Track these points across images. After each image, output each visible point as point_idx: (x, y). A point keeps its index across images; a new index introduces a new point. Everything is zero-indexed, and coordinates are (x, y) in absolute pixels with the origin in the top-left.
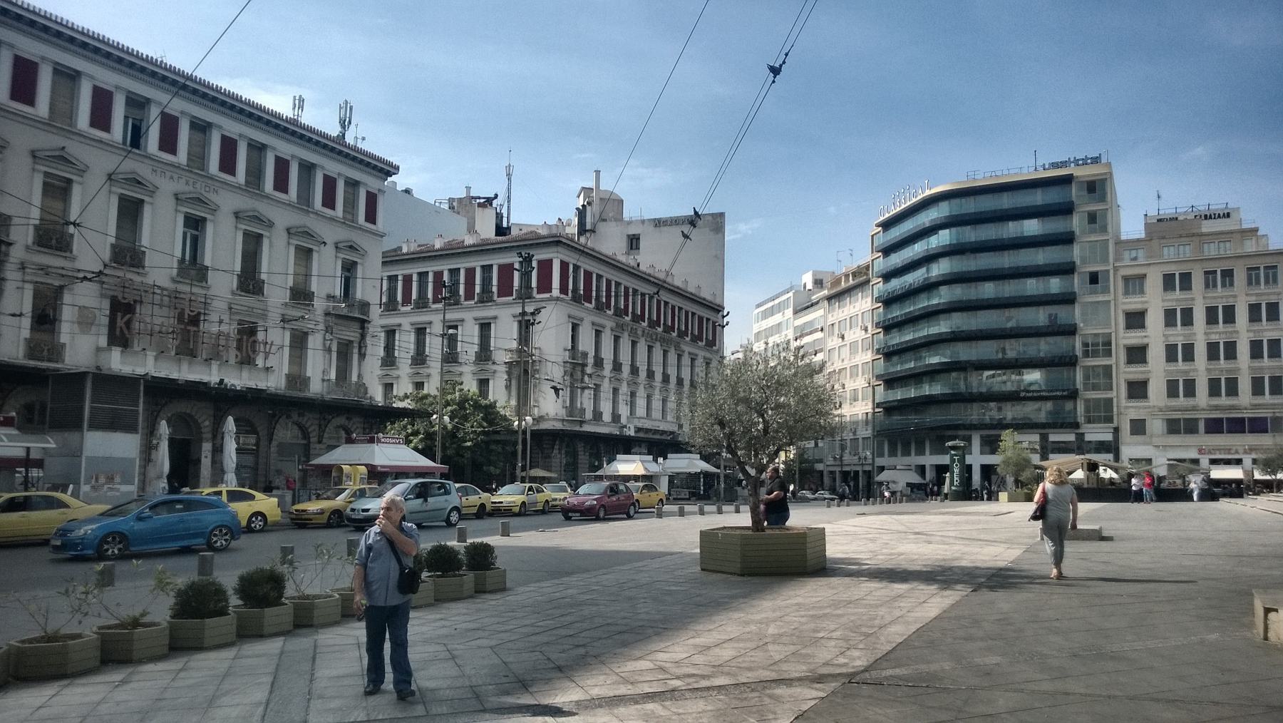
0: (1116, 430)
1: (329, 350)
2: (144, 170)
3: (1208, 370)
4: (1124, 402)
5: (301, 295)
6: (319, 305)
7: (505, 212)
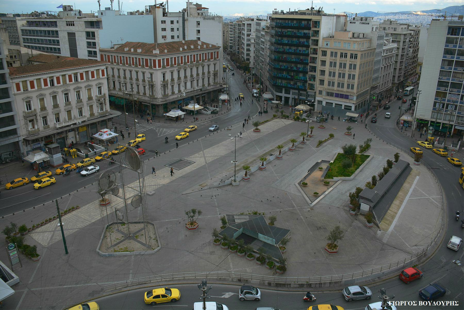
0: (315, 92)
1: (98, 106)
2: (55, 90)
3: (338, 80)
4: (318, 86)
5: (90, 98)
6: (94, 98)
7: (166, 7)
